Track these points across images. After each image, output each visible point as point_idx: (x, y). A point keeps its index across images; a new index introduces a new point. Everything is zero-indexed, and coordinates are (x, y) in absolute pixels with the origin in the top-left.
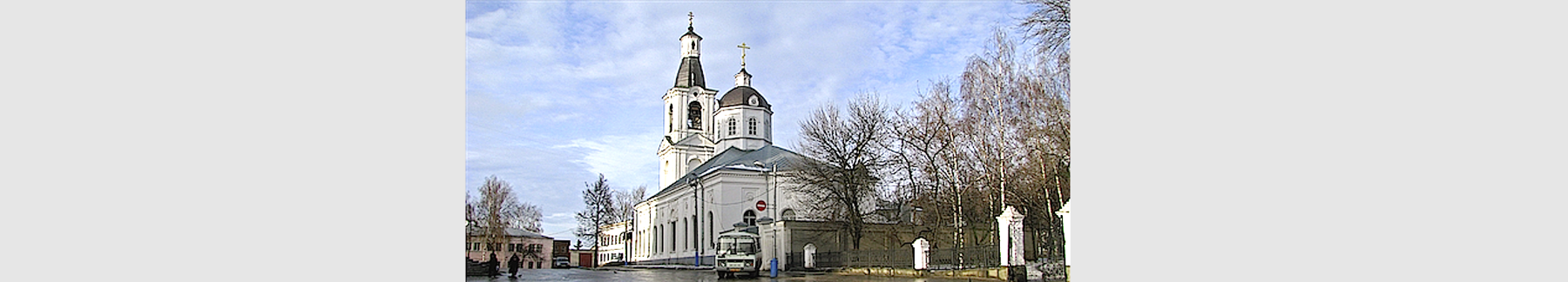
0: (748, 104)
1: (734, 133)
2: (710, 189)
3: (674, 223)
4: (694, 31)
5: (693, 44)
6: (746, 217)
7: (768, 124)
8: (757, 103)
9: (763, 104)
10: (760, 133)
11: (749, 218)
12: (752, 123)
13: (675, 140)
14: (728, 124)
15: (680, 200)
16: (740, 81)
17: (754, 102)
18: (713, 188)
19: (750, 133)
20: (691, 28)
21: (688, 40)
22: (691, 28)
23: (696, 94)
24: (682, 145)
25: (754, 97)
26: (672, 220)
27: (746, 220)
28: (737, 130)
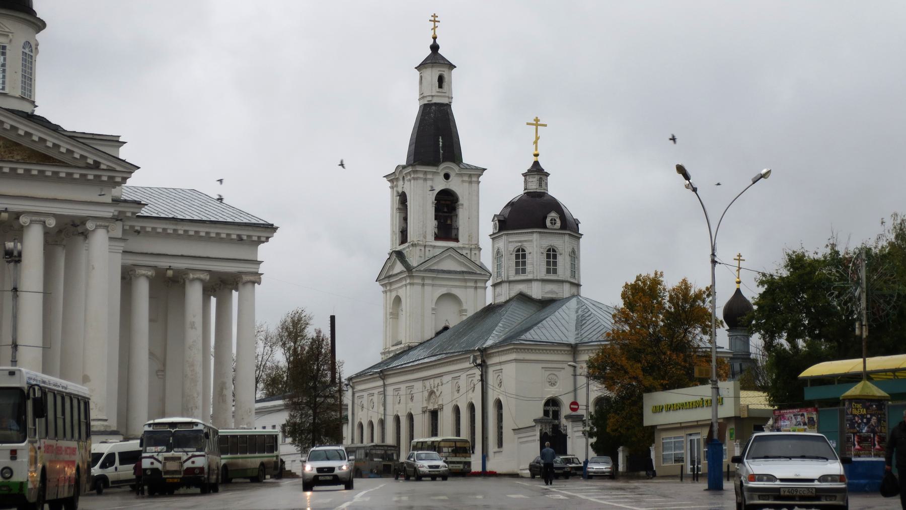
0: (545, 227)
1: (524, 271)
2: (498, 367)
3: (434, 414)
4: (440, 51)
5: (441, 80)
6: (548, 408)
7: (574, 255)
8: (559, 223)
9: (570, 227)
10: (563, 270)
11: (551, 409)
12: (551, 255)
13: (414, 261)
14: (514, 256)
15: (446, 379)
16: (534, 186)
17: (553, 222)
18: (503, 367)
19: (548, 271)
20: (435, 48)
21: (432, 75)
22: (435, 48)
23: (447, 176)
24: (426, 271)
25: (553, 215)
26: (431, 407)
27: (546, 413)
28: (529, 268)
